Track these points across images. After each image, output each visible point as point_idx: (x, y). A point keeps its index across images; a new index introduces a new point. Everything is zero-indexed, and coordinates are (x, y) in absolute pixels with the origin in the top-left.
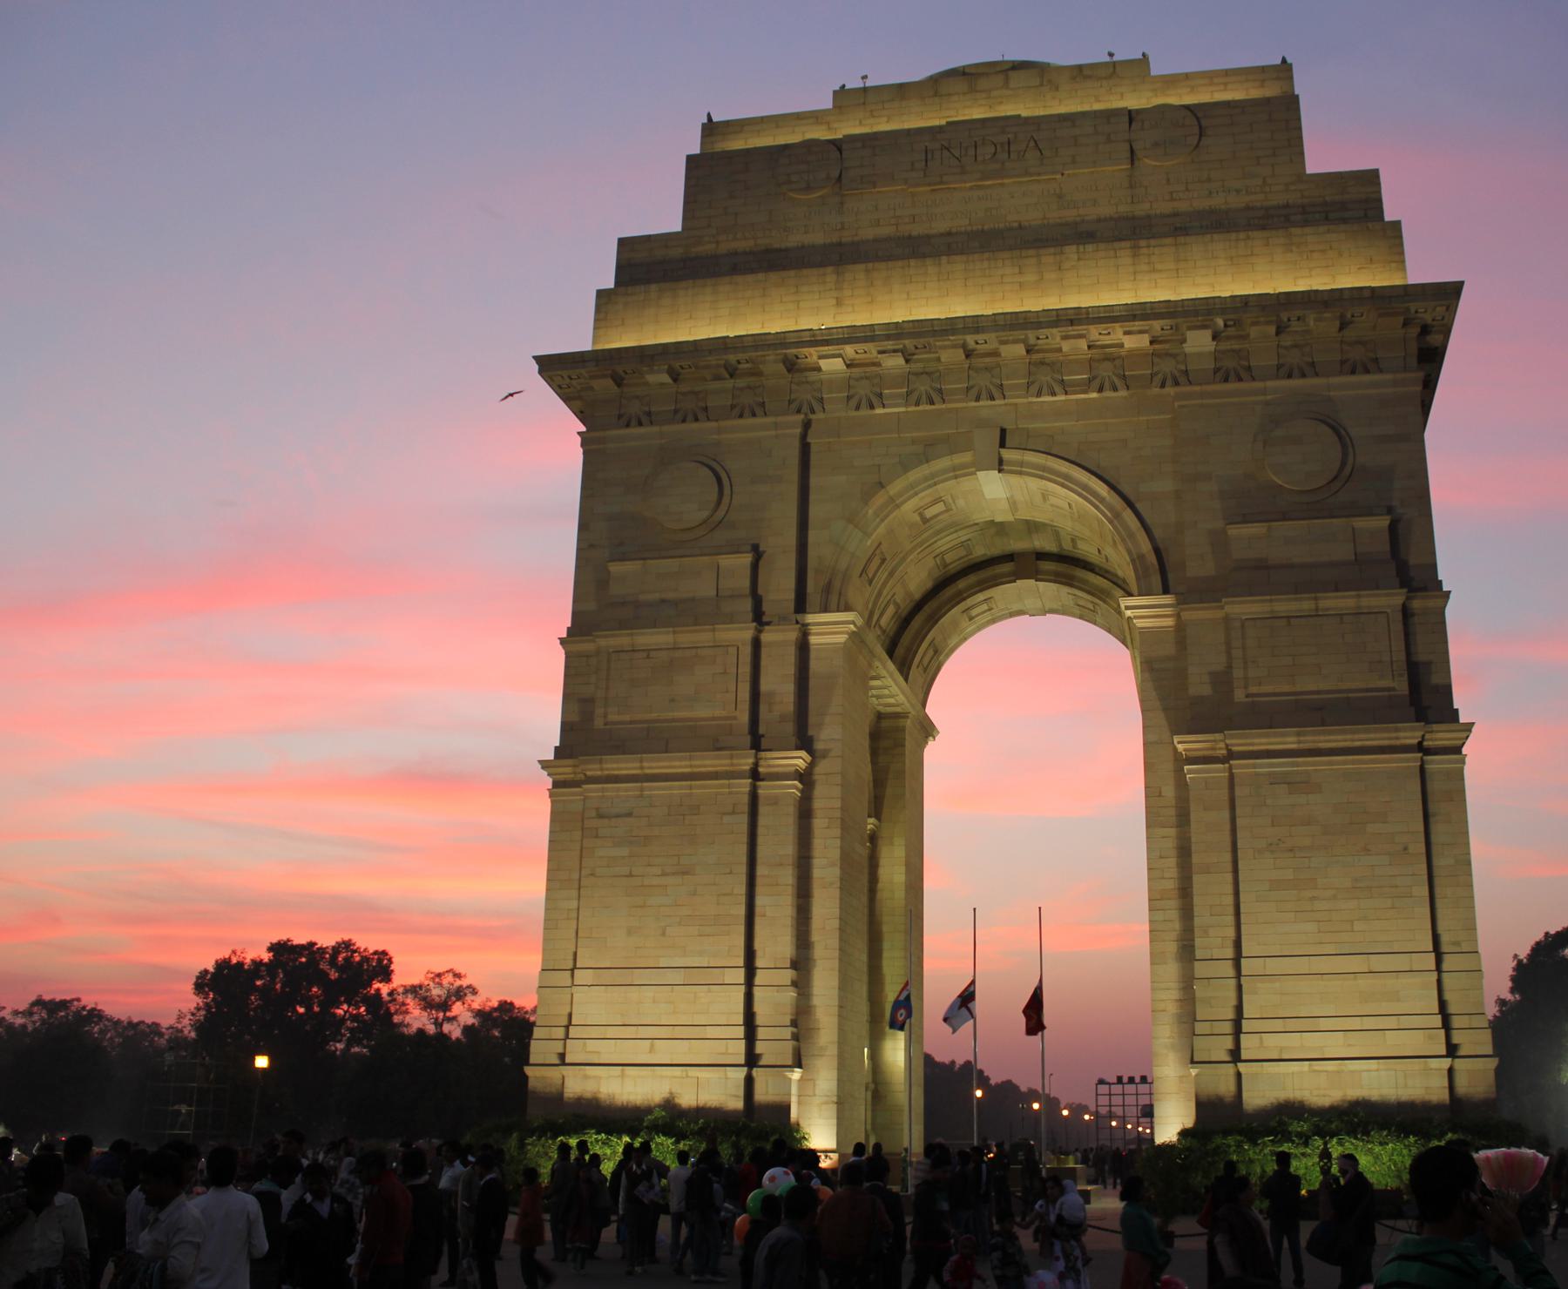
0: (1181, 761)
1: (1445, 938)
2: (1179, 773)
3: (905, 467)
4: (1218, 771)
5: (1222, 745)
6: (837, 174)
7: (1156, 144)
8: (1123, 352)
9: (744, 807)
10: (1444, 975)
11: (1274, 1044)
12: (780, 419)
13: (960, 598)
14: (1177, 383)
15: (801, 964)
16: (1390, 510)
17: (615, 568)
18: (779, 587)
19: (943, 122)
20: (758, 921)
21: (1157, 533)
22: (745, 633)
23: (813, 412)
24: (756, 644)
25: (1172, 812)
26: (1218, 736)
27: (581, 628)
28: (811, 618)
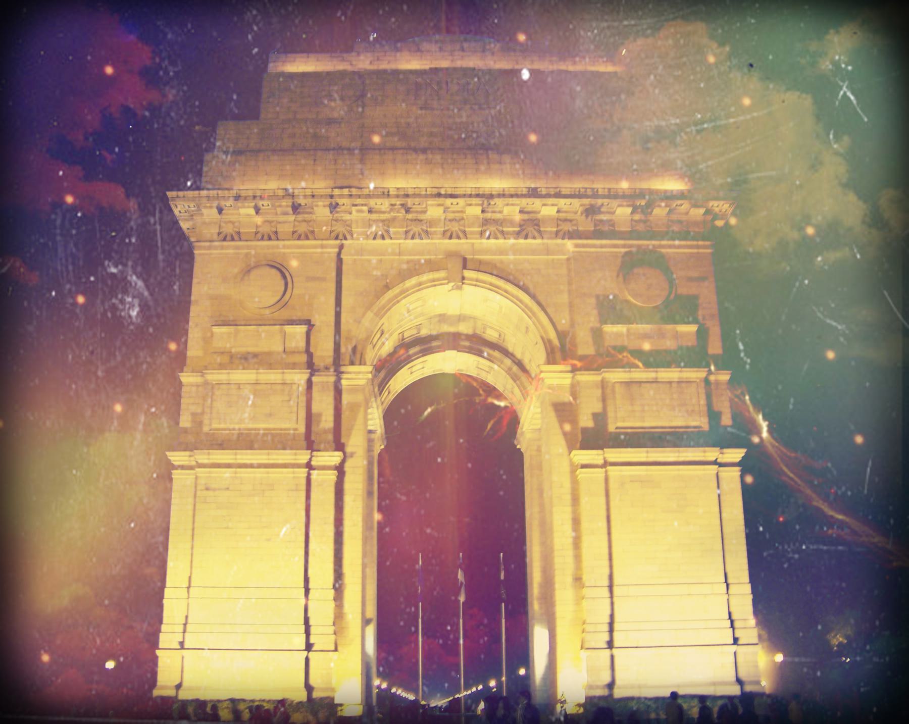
1: (730, 575)
2: (573, 472)
3: (403, 280)
5: (601, 457)
8: (539, 216)
9: (303, 487)
10: (731, 597)
12: (325, 242)
16: (695, 321)
17: (216, 329)
18: (324, 349)
19: (427, 67)
21: (559, 328)
22: (305, 377)
23: (346, 239)
24: (309, 384)
26: (600, 452)
28: (343, 369)
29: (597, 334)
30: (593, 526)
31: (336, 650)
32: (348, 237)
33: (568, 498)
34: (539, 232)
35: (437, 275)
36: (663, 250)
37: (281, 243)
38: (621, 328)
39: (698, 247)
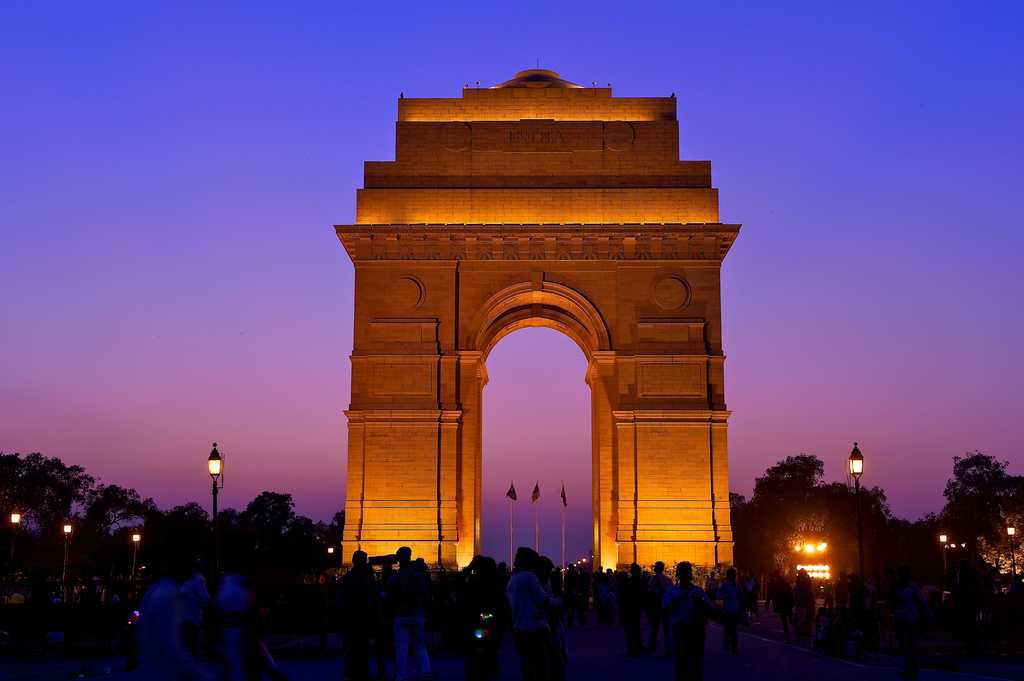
0: (615, 420)
1: (716, 496)
3: (502, 287)
4: (630, 426)
6: (468, 140)
7: (615, 141)
8: (597, 242)
11: (648, 535)
13: (505, 325)
14: (619, 259)
15: (459, 499)
16: (704, 320)
17: (374, 325)
18: (448, 340)
20: (442, 480)
24: (439, 362)
25: (610, 441)
27: (357, 352)
28: (461, 353)
29: (633, 330)
30: (626, 459)
31: (458, 540)
32: (463, 256)
33: (610, 442)
34: (597, 254)
35: (525, 284)
36: (686, 267)
37: (415, 262)
38: (650, 325)
39: (711, 264)
